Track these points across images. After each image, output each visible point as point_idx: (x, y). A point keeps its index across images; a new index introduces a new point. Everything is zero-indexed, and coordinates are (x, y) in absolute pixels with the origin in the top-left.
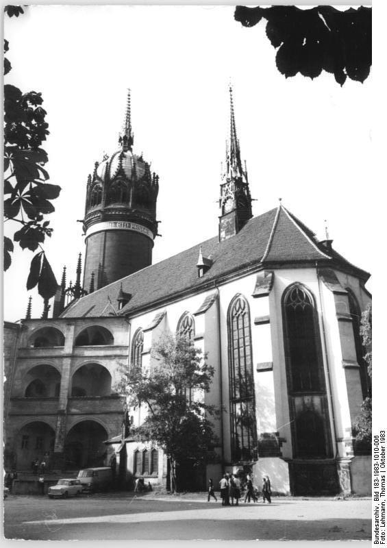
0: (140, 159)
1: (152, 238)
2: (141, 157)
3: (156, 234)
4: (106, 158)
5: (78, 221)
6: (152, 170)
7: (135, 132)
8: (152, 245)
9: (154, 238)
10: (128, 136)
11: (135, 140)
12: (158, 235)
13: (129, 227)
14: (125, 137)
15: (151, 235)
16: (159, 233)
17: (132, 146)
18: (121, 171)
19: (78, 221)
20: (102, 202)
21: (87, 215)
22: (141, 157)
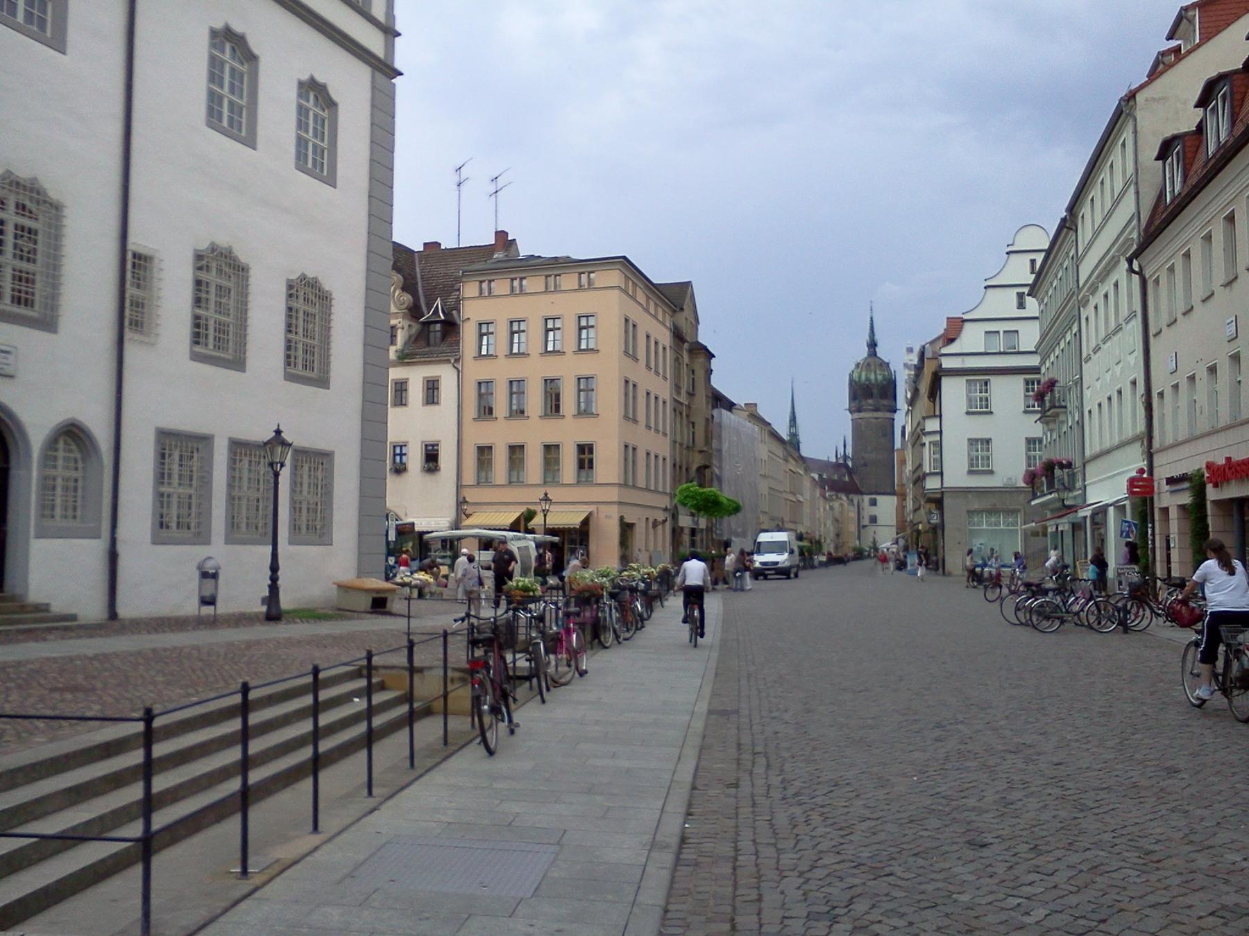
6: (892, 368)
7: (878, 337)
11: (878, 345)
14: (871, 345)
21: (850, 407)
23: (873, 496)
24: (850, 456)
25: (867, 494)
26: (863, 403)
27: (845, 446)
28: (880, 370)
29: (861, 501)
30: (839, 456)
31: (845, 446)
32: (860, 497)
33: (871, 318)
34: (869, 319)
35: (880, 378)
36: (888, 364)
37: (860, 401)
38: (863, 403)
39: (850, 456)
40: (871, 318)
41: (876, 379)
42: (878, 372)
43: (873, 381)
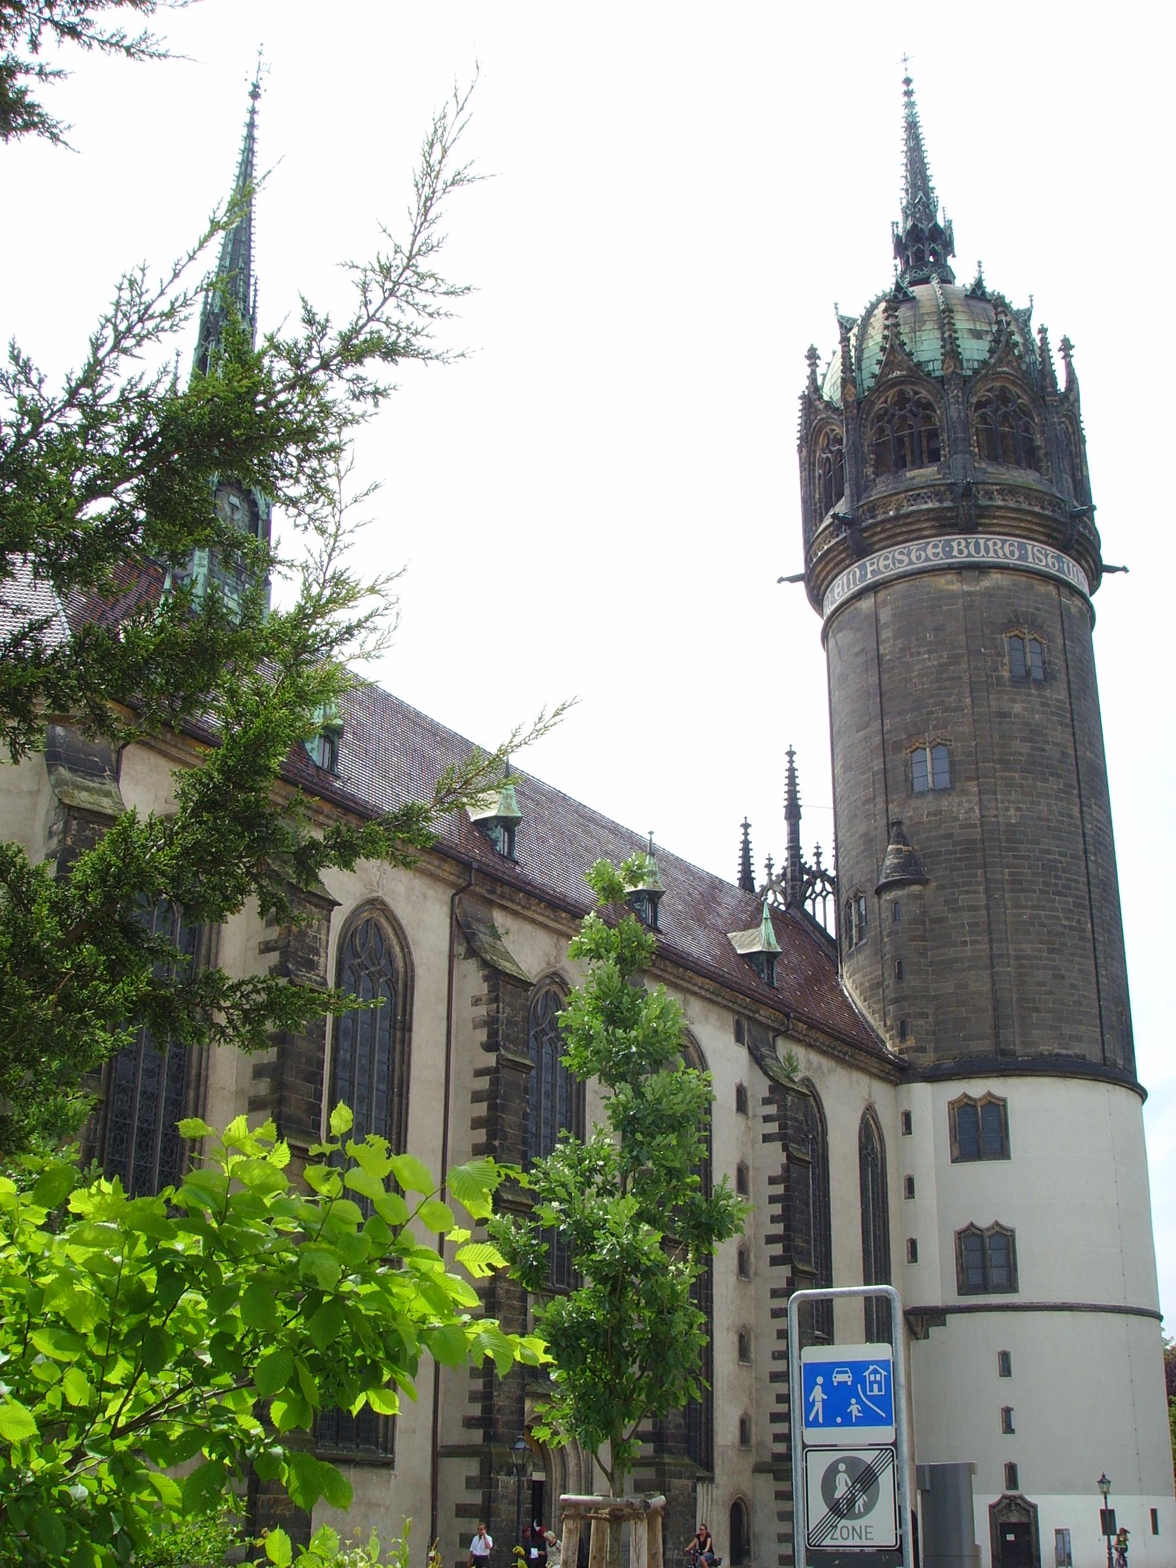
0: (977, 292)
1: (1086, 590)
2: (979, 284)
3: (1096, 570)
4: (845, 325)
5: (781, 580)
8: (1089, 616)
9: (1094, 585)
10: (925, 226)
12: (1112, 570)
13: (949, 555)
15: (1076, 576)
16: (1106, 561)
17: (950, 261)
18: (894, 349)
19: (781, 580)
20: (847, 492)
22: (979, 284)
23: (977, 1088)
24: (828, 864)
25: (933, 1076)
26: (881, 489)
27: (793, 812)
28: (973, 317)
29: (889, 1122)
30: (760, 879)
31: (793, 812)
32: (881, 1093)
33: (912, 127)
34: (899, 134)
35: (974, 350)
36: (1027, 315)
37: (860, 490)
38: (881, 489)
39: (828, 864)
40: (912, 127)
41: (952, 352)
42: (962, 323)
43: (936, 368)
